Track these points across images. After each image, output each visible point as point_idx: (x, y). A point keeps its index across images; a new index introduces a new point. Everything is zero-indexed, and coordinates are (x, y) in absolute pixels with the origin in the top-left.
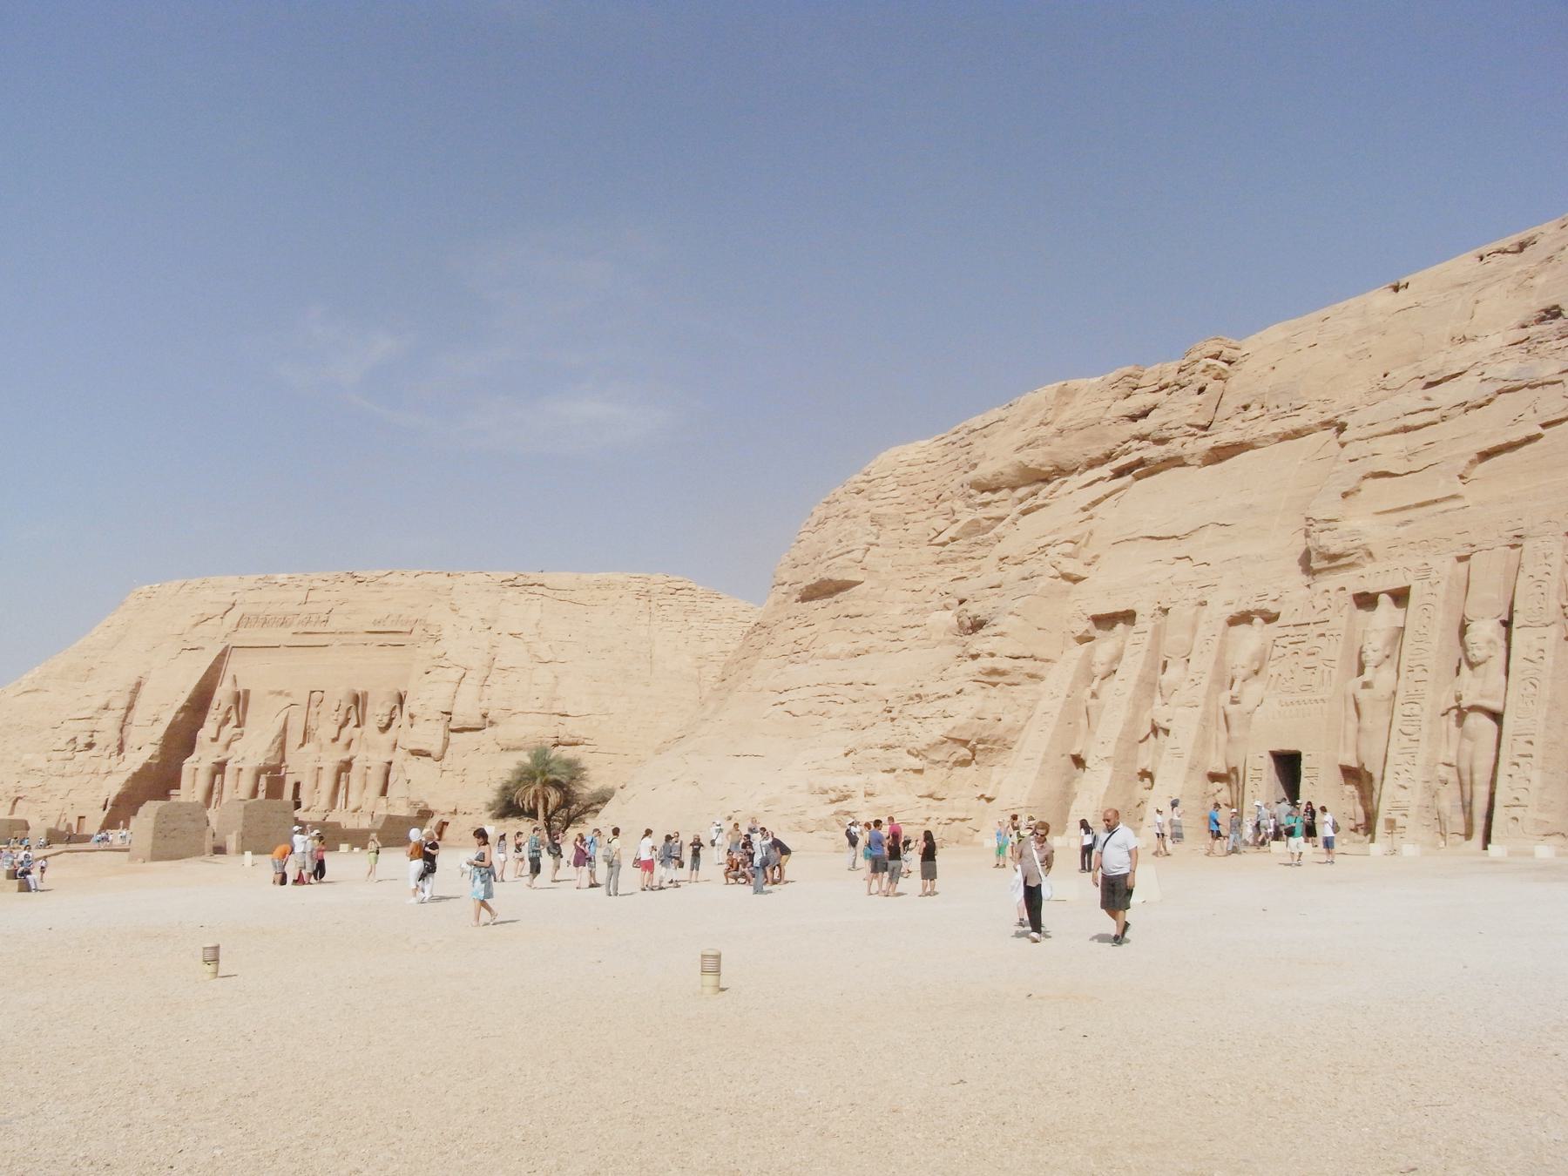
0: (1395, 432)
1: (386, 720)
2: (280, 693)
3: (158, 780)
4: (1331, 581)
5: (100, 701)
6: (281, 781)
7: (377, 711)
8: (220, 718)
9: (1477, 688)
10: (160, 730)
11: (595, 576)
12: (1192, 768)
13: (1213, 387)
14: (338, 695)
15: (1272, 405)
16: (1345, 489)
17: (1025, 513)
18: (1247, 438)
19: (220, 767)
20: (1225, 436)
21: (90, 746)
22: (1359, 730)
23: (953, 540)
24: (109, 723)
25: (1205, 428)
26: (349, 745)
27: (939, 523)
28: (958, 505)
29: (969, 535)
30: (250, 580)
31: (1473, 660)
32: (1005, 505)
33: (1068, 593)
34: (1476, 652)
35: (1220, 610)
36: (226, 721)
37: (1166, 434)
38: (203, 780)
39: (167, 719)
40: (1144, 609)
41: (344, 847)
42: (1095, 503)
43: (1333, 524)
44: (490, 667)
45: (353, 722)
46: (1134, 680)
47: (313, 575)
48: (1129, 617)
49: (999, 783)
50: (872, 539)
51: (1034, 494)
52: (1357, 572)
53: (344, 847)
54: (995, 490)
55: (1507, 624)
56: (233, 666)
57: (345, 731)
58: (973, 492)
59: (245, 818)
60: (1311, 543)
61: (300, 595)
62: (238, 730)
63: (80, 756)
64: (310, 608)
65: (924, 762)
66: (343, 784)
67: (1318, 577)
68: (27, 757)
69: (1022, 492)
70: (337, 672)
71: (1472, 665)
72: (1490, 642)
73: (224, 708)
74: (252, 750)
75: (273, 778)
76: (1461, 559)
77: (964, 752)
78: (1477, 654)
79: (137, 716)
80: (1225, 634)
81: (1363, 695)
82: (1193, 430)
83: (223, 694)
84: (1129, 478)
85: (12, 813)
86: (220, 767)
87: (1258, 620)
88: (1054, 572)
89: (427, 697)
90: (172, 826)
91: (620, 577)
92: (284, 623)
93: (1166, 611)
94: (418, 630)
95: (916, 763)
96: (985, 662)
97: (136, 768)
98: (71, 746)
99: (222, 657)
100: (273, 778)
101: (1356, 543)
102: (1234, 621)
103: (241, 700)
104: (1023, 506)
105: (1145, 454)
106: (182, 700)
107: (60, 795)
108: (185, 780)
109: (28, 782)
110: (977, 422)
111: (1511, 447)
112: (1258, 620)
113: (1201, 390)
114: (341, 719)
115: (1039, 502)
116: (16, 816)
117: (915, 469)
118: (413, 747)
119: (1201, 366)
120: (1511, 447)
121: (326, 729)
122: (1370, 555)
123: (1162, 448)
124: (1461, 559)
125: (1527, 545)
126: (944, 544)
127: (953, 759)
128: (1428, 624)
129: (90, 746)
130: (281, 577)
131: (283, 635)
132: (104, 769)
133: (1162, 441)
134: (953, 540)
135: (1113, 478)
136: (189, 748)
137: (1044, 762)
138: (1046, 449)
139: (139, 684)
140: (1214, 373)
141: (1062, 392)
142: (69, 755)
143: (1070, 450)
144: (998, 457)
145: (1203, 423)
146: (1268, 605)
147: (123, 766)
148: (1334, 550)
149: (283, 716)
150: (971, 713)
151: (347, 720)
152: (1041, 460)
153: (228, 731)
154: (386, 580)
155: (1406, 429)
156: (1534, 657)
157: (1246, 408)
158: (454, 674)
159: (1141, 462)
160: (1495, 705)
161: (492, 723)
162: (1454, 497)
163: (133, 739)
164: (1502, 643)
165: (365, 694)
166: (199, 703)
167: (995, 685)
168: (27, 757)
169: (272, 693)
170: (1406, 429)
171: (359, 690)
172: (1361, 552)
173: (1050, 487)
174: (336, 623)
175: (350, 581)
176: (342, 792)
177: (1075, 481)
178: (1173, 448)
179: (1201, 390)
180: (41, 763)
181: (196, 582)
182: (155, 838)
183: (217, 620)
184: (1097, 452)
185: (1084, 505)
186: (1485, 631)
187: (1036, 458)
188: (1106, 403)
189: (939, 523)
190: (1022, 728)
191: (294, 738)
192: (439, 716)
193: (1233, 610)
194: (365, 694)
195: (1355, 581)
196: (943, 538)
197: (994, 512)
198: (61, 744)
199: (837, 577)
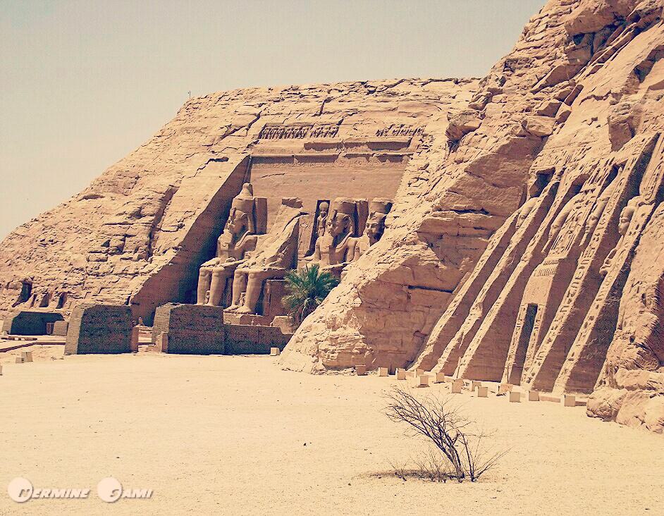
3: (182, 284)
5: (131, 209)
10: (182, 234)
14: (337, 200)
19: (228, 275)
21: (120, 250)
24: (139, 229)
39: (189, 224)
40: (558, 171)
41: (274, 350)
50: (496, 85)
53: (274, 350)
59: (172, 320)
61: (314, 105)
63: (111, 259)
64: (324, 118)
68: (76, 257)
70: (341, 185)
74: (265, 252)
79: (168, 221)
85: (61, 305)
90: (98, 326)
92: (300, 135)
94: (416, 140)
98: (106, 249)
107: (93, 291)
121: (325, 240)
129: (120, 250)
131: (294, 146)
132: (131, 271)
139: (171, 193)
142: (103, 256)
147: (150, 266)
150: (402, 261)
154: (394, 89)
166: (219, 210)
168: (76, 257)
169: (285, 202)
174: (343, 135)
180: (83, 264)
183: (242, 132)
189: (546, 67)
191: (304, 247)
198: (97, 247)
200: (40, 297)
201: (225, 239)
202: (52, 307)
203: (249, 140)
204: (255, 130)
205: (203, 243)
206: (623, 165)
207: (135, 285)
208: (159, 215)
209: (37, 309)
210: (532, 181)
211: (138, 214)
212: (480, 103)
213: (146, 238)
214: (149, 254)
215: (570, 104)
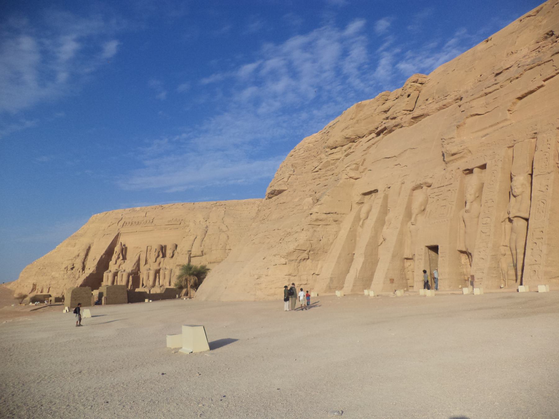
0: (481, 96)
1: (171, 255)
2: (137, 247)
4: (453, 166)
5: (76, 253)
6: (139, 277)
7: (169, 253)
8: (116, 257)
9: (517, 207)
10: (96, 262)
11: (244, 201)
12: (393, 256)
13: (414, 94)
14: (155, 246)
15: (436, 97)
16: (459, 124)
17: (346, 156)
18: (425, 112)
19: (116, 274)
20: (416, 113)
21: (72, 269)
22: (465, 232)
23: (320, 169)
25: (410, 111)
26: (160, 264)
27: (316, 164)
28: (323, 156)
29: (326, 167)
30: (128, 209)
31: (515, 194)
32: (339, 154)
33: (353, 185)
34: (516, 190)
35: (410, 185)
36: (118, 258)
37: (395, 116)
38: (110, 279)
39: (98, 258)
40: (380, 188)
42: (368, 148)
43: (453, 140)
44: (205, 235)
45: (161, 255)
46: (374, 220)
47: (149, 207)
48: (376, 191)
49: (322, 268)
50: (292, 173)
51: (350, 148)
52: (464, 160)
53: (146, 300)
54: (336, 148)
55: (531, 175)
56: (122, 240)
57: (158, 260)
58: (327, 150)
60: (444, 150)
62: (123, 261)
65: (287, 261)
66: (157, 277)
67: (448, 165)
68: (53, 273)
69: (345, 147)
71: (515, 196)
72: (522, 185)
73: (117, 253)
74: (128, 266)
75: (135, 276)
76: (509, 147)
77: (305, 255)
78: (516, 191)
79: (90, 257)
80: (411, 195)
81: (466, 216)
82: (406, 112)
83: (117, 249)
84: (382, 135)
85: (48, 292)
86: (116, 274)
87: (425, 187)
88: (346, 177)
89: (184, 247)
91: (252, 200)
93: (389, 188)
95: (283, 261)
96: (314, 217)
97: (87, 275)
99: (117, 237)
100: (135, 276)
101: (462, 148)
102: (415, 189)
103: (124, 250)
104: (346, 153)
105: (386, 125)
106: (103, 252)
108: (105, 279)
109: (53, 282)
110: (331, 123)
111: (531, 92)
112: (425, 187)
113: (409, 96)
114: (157, 255)
115: (351, 151)
116: (50, 293)
117: (311, 145)
118: (177, 264)
119: (409, 86)
120: (531, 92)
122: (470, 152)
123: (394, 121)
124: (509, 147)
125: (539, 136)
126: (317, 171)
127: (299, 258)
128: (494, 179)
129: (72, 269)
130: (138, 208)
133: (394, 118)
134: (320, 169)
135: (377, 136)
136: (106, 267)
137: (339, 257)
138: (352, 129)
139: (90, 248)
140: (414, 88)
141: (358, 106)
143: (363, 128)
144: (337, 136)
145: (411, 109)
146: (429, 181)
148: (453, 152)
149: (138, 255)
151: (158, 256)
152: (350, 134)
153: (119, 261)
155: (486, 94)
156: (543, 189)
157: (427, 100)
158: (192, 238)
159: (385, 129)
160: (526, 216)
161: (205, 254)
162: (506, 120)
163: (87, 266)
164: (528, 185)
165: (165, 247)
166: (109, 253)
167: (319, 225)
168: (53, 273)
170: (486, 94)
171: (163, 244)
172: (466, 151)
173: (355, 144)
175: (160, 208)
176: (157, 280)
177: (365, 139)
178: (397, 121)
179: (409, 96)
180: (57, 275)
181: (111, 212)
182: (71, 300)
184: (372, 128)
185: (364, 149)
186: (521, 180)
187: (349, 133)
188: (375, 108)
190: (332, 243)
191: (142, 263)
192: (186, 252)
193: (414, 185)
194: (165, 247)
195: (463, 164)
196: (316, 169)
197: (335, 156)
199: (277, 189)
200: (40, 290)
201: (111, 263)
202: (45, 293)
203: (119, 227)
204: (121, 223)
205: (103, 264)
206: (483, 167)
207: (80, 282)
208: (87, 255)
209: (39, 293)
210: (358, 198)
211: (78, 256)
212: (285, 179)
213: (82, 265)
214: (83, 269)
215: (362, 165)
